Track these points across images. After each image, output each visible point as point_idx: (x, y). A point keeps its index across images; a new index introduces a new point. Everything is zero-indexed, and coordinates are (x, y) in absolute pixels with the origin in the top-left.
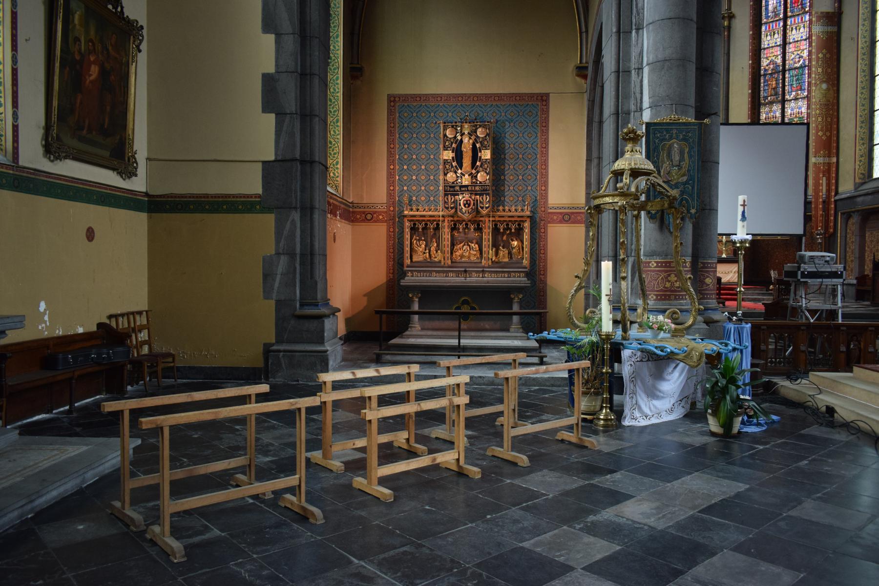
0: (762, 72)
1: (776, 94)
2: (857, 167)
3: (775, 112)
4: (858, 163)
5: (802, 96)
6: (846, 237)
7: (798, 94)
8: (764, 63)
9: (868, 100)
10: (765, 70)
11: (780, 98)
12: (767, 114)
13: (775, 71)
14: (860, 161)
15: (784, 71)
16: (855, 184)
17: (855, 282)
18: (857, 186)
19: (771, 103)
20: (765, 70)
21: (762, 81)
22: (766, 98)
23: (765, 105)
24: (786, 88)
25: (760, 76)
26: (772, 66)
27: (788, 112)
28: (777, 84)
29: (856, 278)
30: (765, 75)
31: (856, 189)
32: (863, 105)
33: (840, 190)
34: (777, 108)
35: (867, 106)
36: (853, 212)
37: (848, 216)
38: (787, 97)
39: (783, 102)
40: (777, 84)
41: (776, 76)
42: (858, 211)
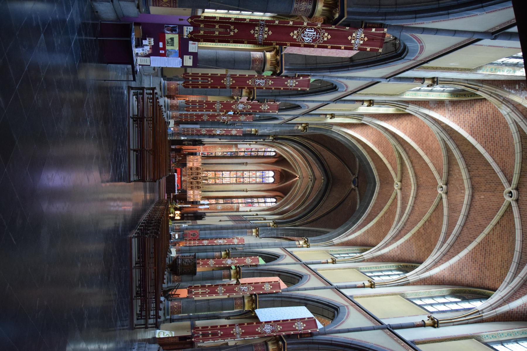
8: (234, 200)
34: (222, 202)
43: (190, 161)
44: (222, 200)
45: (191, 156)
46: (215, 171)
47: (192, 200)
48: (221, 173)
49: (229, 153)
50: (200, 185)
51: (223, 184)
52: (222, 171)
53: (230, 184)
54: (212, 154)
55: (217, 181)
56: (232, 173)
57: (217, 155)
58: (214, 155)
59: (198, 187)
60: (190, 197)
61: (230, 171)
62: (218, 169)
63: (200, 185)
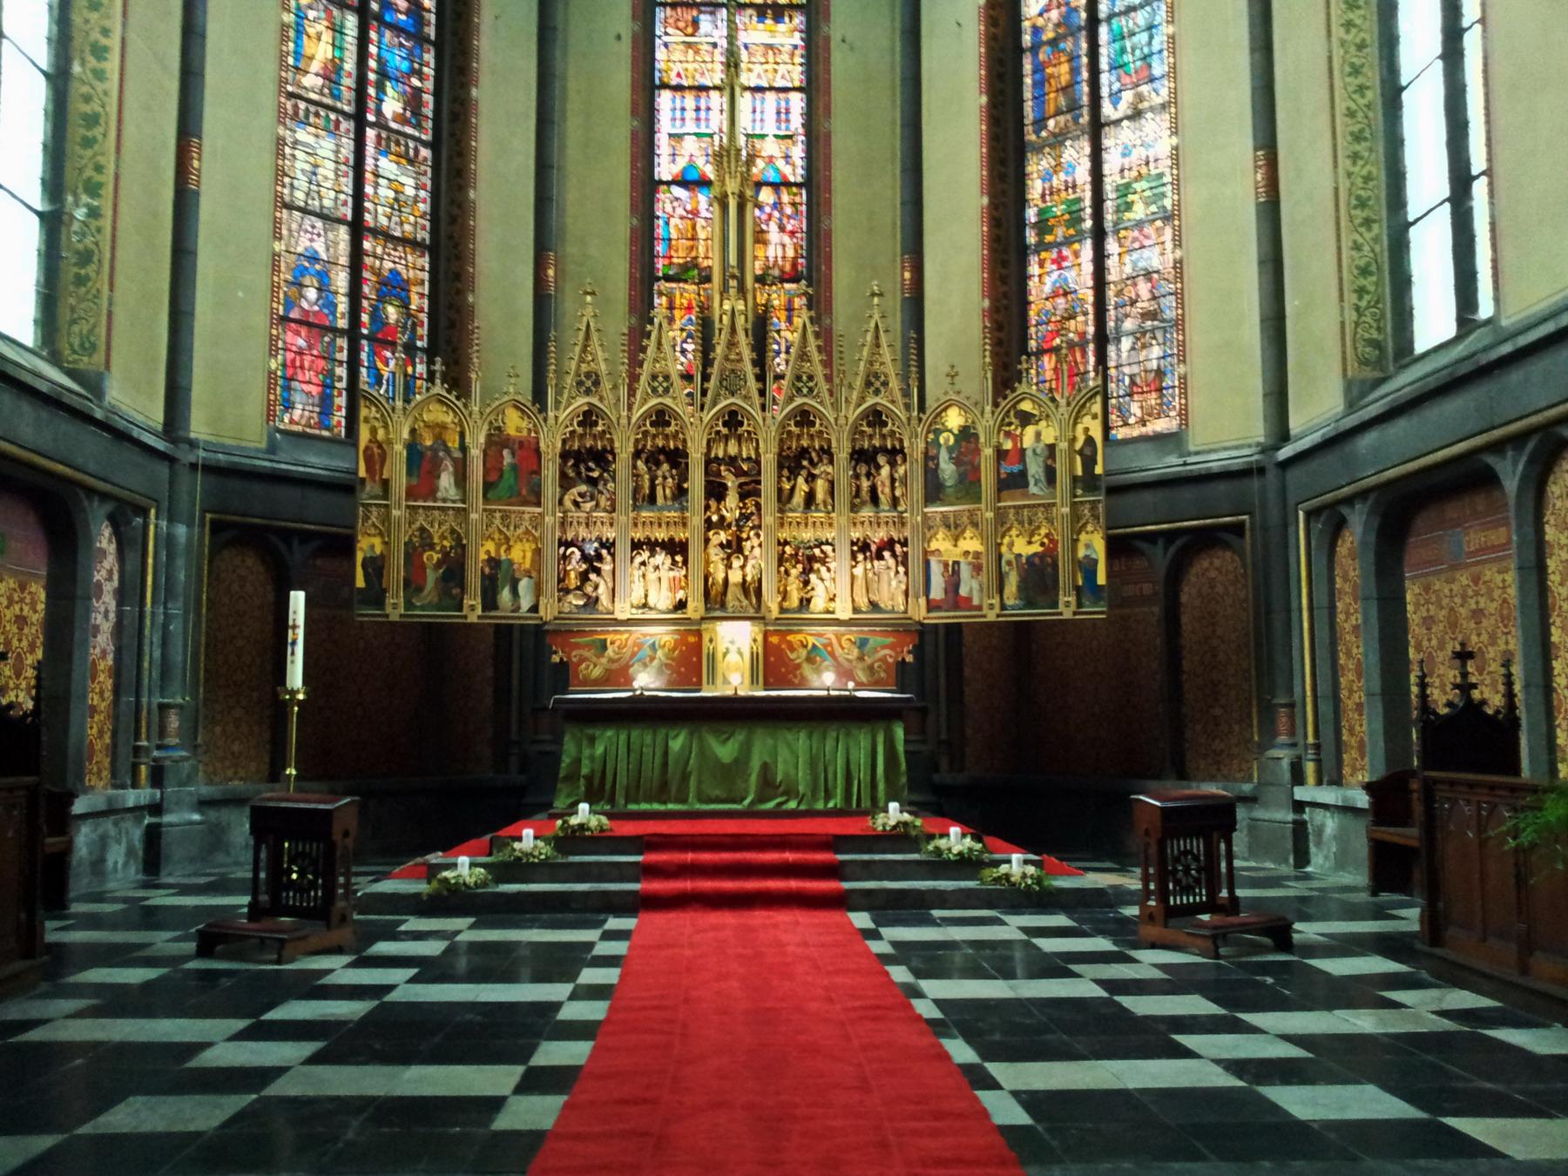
0: (1027, 39)
1: (1073, 107)
2: (1351, 316)
3: (1072, 168)
4: (1351, 298)
5: (1158, 100)
6: (1332, 609)
7: (1140, 98)
9: (1373, 51)
10: (1036, 30)
11: (1085, 119)
12: (1046, 178)
13: (1066, 27)
14: (1361, 291)
15: (1093, 22)
16: (1349, 385)
17: (1362, 800)
18: (1355, 393)
19: (1058, 140)
20: (1036, 30)
21: (1027, 67)
22: (1040, 123)
23: (1039, 150)
24: (1104, 78)
25: (1019, 51)
26: (1054, 15)
27: (1112, 163)
28: (1074, 71)
29: (1369, 787)
30: (1035, 49)
31: (1352, 405)
32: (1356, 71)
33: (1295, 423)
34: (1077, 155)
35: (1372, 76)
36: (1349, 501)
37: (1331, 520)
38: (1107, 110)
39: (1097, 128)
40: (1074, 71)
41: (1068, 45)
42: (1363, 494)
43: (454, 570)
44: (1037, 166)
45: (368, 545)
46: (644, 280)
47: (1094, 544)
48: (672, 205)
49: (390, 50)
50: (840, 421)
51: (816, 182)
52: (646, 187)
53: (815, 86)
54: (394, 287)
55: (779, 246)
56: (671, 58)
57: (415, 224)
58: (416, 268)
59: (863, 457)
60: (1039, 577)
61: (647, 84)
62: (623, 223)
63: (840, 421)
